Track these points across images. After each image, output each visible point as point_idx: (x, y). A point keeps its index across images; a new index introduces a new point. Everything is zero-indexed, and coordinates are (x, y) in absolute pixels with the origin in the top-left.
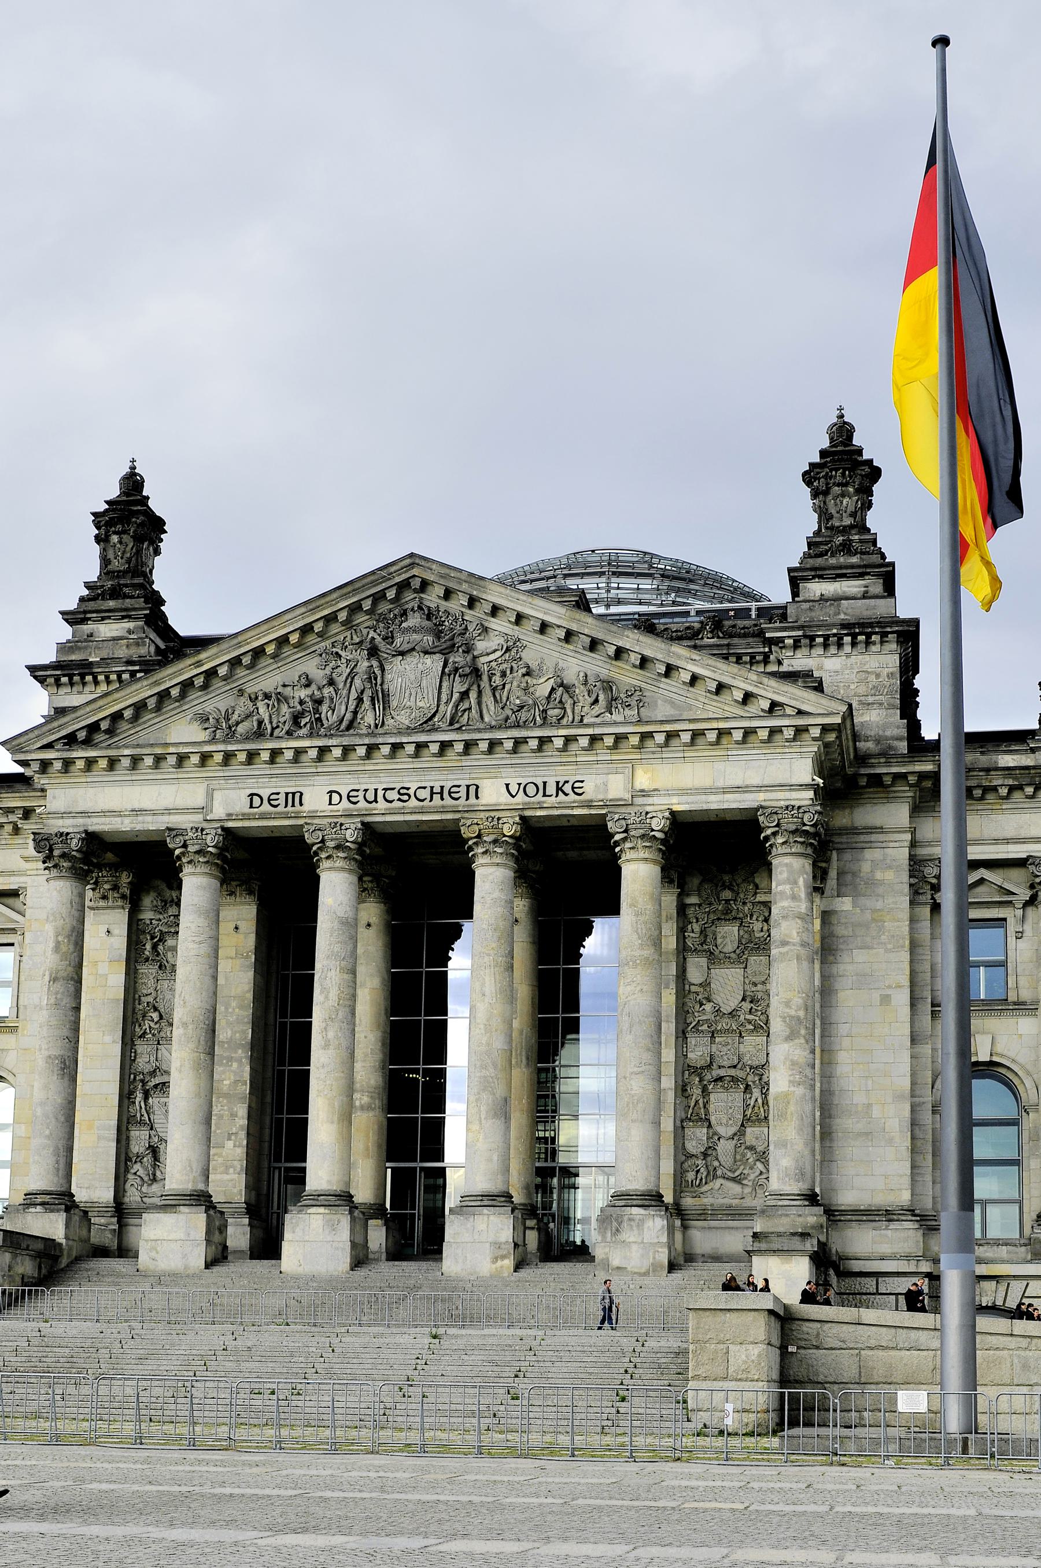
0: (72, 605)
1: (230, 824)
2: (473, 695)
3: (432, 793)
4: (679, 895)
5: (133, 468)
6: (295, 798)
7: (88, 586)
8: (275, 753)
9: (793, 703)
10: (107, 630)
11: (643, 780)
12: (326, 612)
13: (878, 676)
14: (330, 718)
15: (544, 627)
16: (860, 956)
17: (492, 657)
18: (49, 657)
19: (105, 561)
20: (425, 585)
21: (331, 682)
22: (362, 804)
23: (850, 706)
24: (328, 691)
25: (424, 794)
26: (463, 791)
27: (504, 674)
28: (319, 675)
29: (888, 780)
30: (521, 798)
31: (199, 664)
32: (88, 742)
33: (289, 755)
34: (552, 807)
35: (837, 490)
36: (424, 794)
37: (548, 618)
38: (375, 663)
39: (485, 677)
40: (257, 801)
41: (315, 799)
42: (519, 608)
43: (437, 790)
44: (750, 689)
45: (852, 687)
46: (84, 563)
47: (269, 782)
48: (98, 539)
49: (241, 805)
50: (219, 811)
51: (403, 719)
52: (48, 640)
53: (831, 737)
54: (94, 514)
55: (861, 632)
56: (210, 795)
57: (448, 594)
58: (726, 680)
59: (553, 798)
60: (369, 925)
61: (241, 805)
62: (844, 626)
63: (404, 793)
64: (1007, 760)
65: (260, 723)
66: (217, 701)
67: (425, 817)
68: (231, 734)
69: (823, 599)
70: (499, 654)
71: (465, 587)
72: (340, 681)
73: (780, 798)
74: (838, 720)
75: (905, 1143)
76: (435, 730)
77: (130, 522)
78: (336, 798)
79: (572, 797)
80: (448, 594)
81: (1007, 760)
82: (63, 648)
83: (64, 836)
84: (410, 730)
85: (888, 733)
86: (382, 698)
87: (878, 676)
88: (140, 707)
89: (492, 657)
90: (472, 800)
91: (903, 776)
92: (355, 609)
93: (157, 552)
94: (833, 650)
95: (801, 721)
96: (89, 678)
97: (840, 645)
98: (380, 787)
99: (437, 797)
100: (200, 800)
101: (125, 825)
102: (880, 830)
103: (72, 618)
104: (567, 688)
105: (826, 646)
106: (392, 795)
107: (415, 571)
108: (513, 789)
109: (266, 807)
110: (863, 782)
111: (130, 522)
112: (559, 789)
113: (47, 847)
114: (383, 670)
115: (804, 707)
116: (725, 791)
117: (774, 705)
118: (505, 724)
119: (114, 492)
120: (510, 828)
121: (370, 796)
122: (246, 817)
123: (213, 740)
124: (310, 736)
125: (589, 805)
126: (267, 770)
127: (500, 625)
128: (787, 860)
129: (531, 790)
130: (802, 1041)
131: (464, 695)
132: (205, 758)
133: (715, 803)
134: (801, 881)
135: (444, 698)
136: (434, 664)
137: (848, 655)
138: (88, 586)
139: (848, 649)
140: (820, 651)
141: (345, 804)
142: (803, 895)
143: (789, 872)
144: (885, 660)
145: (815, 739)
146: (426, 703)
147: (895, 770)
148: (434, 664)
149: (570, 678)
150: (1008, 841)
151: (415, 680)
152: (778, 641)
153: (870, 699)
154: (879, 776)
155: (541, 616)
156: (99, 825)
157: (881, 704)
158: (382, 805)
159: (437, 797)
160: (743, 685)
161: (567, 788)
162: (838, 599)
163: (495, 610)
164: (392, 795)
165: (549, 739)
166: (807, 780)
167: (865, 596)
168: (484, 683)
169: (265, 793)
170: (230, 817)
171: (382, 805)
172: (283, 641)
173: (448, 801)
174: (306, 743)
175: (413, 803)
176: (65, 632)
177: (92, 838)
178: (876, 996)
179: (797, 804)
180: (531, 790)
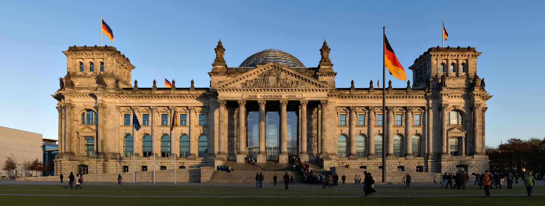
0: (213, 63)
6: (256, 96)
10: (219, 67)
11: (304, 96)
34: (292, 99)
41: (259, 96)
46: (214, 56)
47: (252, 94)
49: (248, 97)
50: (244, 97)
52: (210, 69)
61: (248, 97)
63: (271, 96)
101: (231, 99)
133: (314, 99)
152: (318, 75)
162: (326, 69)
176: (212, 68)
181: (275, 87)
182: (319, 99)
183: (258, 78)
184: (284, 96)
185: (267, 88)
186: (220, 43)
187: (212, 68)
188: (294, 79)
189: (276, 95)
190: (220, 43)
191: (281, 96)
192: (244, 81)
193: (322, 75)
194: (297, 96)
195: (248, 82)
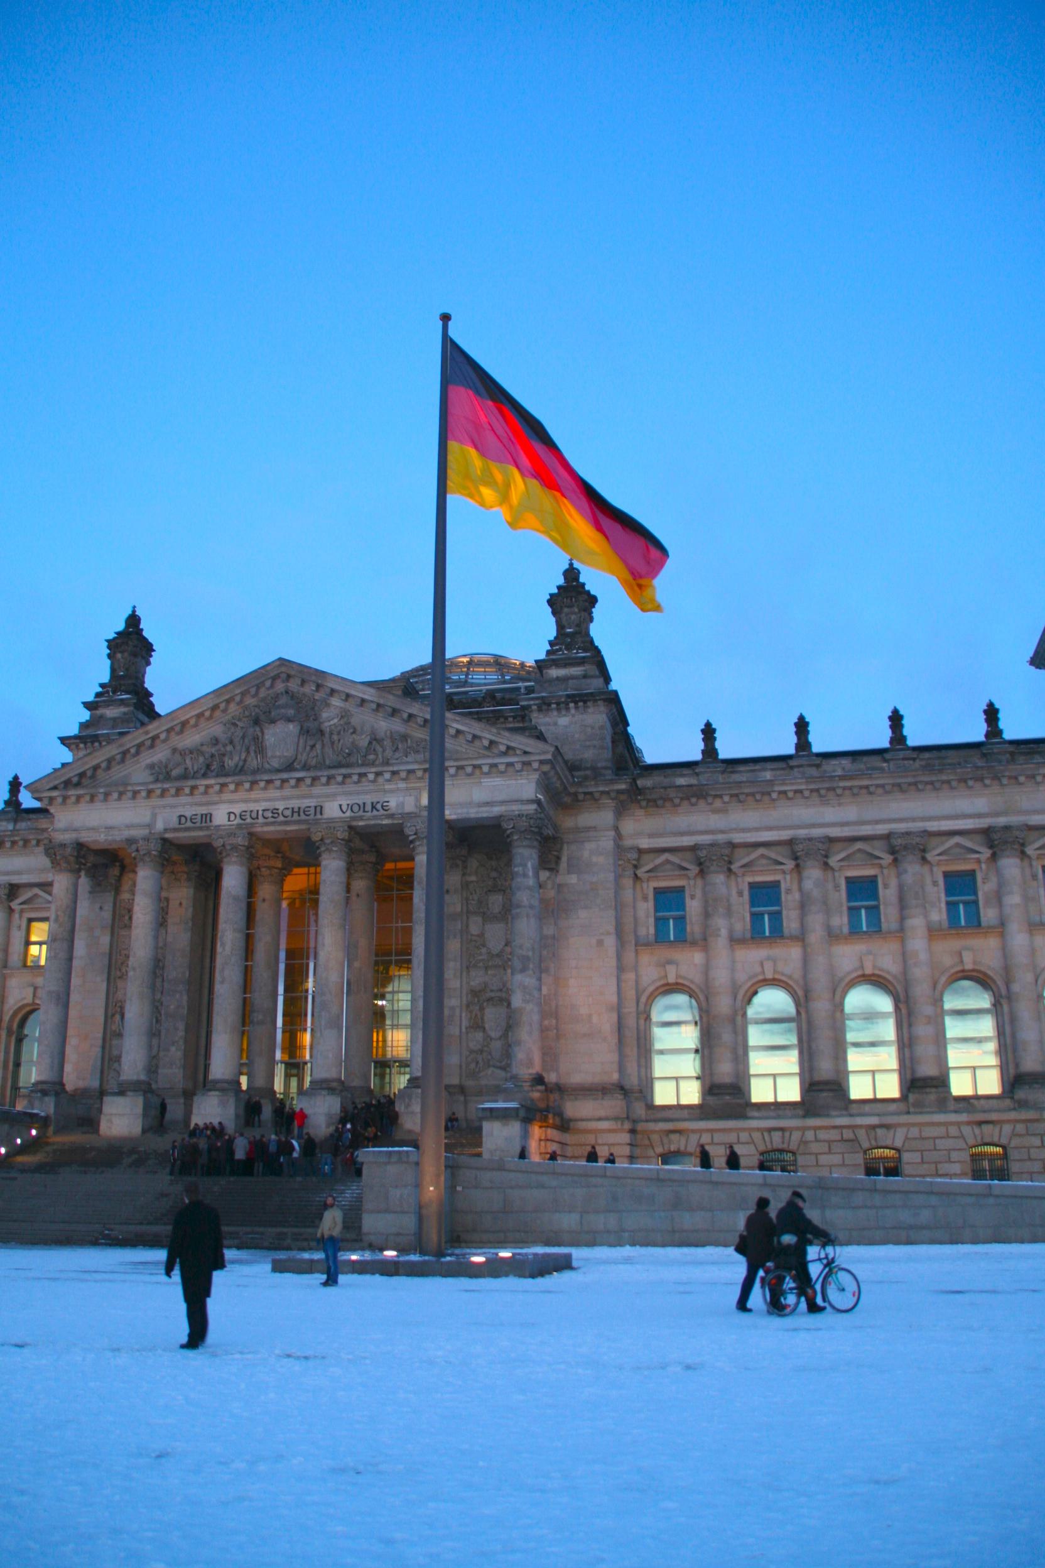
0: (90, 698)
1: (167, 836)
2: (318, 746)
3: (293, 812)
4: (464, 875)
5: (134, 611)
7: (102, 686)
8: (193, 788)
9: (521, 747)
12: (227, 697)
13: (593, 728)
14: (230, 763)
15: (363, 701)
16: (583, 914)
17: (332, 722)
18: (74, 730)
19: (113, 670)
20: (289, 676)
21: (231, 742)
22: (249, 820)
23: (557, 747)
24: (229, 748)
25: (288, 813)
26: (312, 810)
27: (339, 733)
28: (223, 738)
29: (597, 795)
30: (349, 813)
31: (147, 733)
32: (78, 785)
33: (202, 789)
35: (566, 610)
36: (288, 813)
37: (366, 697)
38: (258, 729)
39: (327, 735)
40: (183, 820)
42: (347, 691)
43: (296, 810)
44: (493, 738)
45: (577, 736)
47: (188, 806)
48: (109, 656)
50: (160, 826)
51: (275, 764)
53: (546, 768)
54: (107, 641)
55: (581, 699)
56: (154, 816)
57: (303, 682)
58: (478, 733)
59: (369, 814)
60: (264, 900)
62: (568, 696)
63: (275, 811)
64: (681, 781)
65: (186, 769)
66: (160, 754)
67: (289, 828)
68: (168, 778)
69: (558, 678)
70: (336, 721)
71: (313, 678)
72: (236, 740)
73: (516, 808)
74: (549, 757)
75: (613, 1040)
76: (295, 770)
77: (131, 646)
78: (232, 816)
79: (382, 812)
80: (303, 682)
81: (681, 781)
82: (83, 726)
83: (63, 846)
84: (279, 771)
85: (599, 765)
86: (261, 749)
87: (593, 728)
88: (110, 761)
89: (332, 722)
90: (319, 816)
91: (608, 793)
92: (243, 694)
93: (149, 663)
94: (564, 712)
95: (526, 759)
96: (97, 744)
97: (568, 709)
98: (260, 809)
99: (296, 815)
100: (147, 819)
102: (594, 828)
103: (88, 705)
104: (379, 741)
105: (558, 710)
106: (269, 814)
107: (283, 669)
108: (344, 808)
109: (189, 824)
110: (581, 797)
111: (131, 646)
112: (373, 807)
113: (52, 851)
114: (263, 733)
115: (528, 749)
116: (480, 805)
117: (509, 748)
118: (340, 765)
119: (121, 626)
120: (342, 834)
121: (254, 815)
122: (175, 830)
123: (157, 781)
124: (217, 776)
125: (392, 816)
126: (188, 799)
127: (336, 702)
128: (520, 850)
129: (356, 808)
130: (531, 972)
131: (313, 746)
132: (150, 792)
134: (529, 865)
135: (300, 750)
136: (292, 728)
137: (573, 716)
138: (102, 686)
139: (573, 711)
140: (555, 713)
141: (238, 821)
142: (531, 874)
143: (526, 857)
144: (597, 717)
145: (536, 770)
146: (289, 753)
147: (601, 789)
148: (292, 728)
149: (381, 734)
150: (682, 834)
151: (281, 738)
153: (588, 743)
154: (591, 793)
155: (361, 695)
156: (86, 837)
157: (595, 746)
158: (261, 820)
159: (296, 815)
160: (488, 736)
161: (379, 806)
162: (564, 679)
163: (333, 692)
164: (269, 814)
165: (365, 775)
166: (532, 797)
167: (585, 677)
168: (326, 740)
169: (188, 814)
170: (166, 830)
171: (261, 820)
172: (200, 716)
173: (303, 817)
174: (212, 781)
175: (281, 818)
176: (85, 715)
177: (80, 846)
178: (594, 941)
179: (525, 813)
180: (356, 808)
181: (290, 768)
182: (497, 810)
183: (223, 738)
184: (332, 810)
185: (247, 774)
186: (133, 621)
187: (85, 715)
188: (384, 725)
189: (295, 803)
190: (133, 621)
191: (319, 809)
192: (160, 754)
193: (545, 705)
194: (393, 803)
195: (177, 757)
